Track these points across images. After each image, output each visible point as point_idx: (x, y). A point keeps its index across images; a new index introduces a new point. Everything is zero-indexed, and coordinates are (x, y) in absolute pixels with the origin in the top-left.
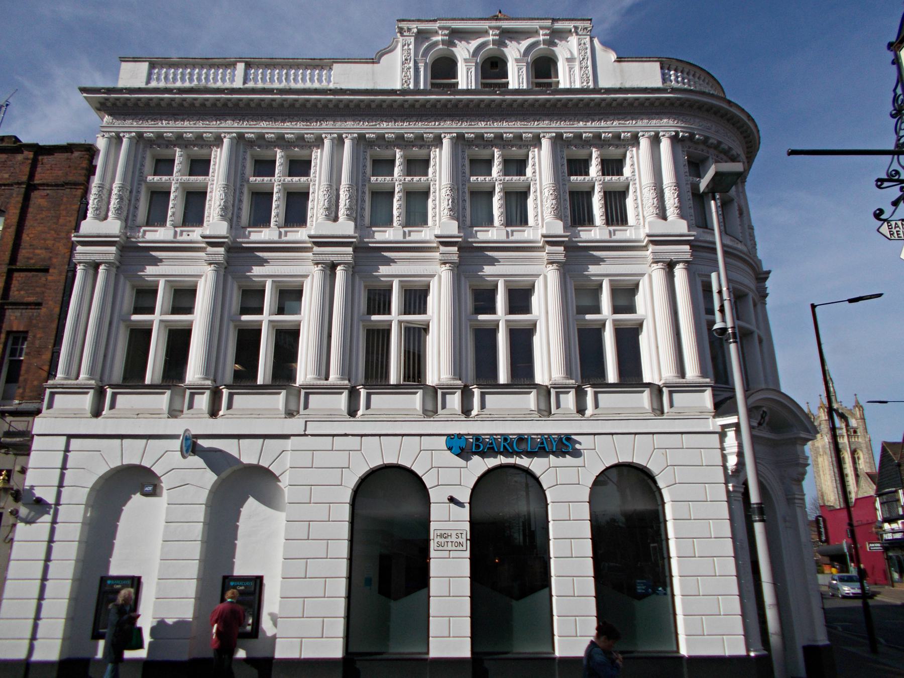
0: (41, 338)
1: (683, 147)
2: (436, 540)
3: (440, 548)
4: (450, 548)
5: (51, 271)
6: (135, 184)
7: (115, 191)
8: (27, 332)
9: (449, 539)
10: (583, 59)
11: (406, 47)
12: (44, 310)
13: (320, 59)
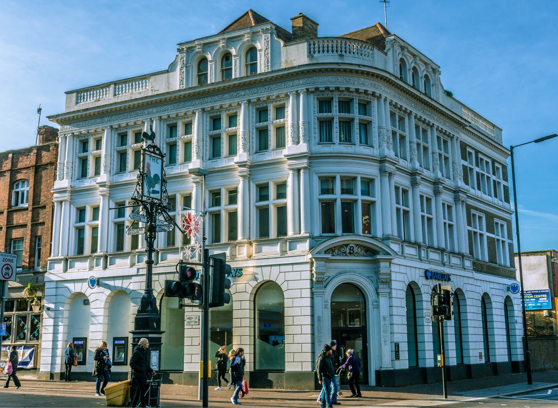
0: (45, 238)
1: (314, 96)
2: (187, 320)
3: (188, 324)
4: (192, 324)
5: (47, 206)
6: (74, 159)
7: (66, 164)
8: (41, 236)
9: (192, 320)
10: (266, 49)
11: (182, 60)
12: (46, 225)
13: (145, 75)
